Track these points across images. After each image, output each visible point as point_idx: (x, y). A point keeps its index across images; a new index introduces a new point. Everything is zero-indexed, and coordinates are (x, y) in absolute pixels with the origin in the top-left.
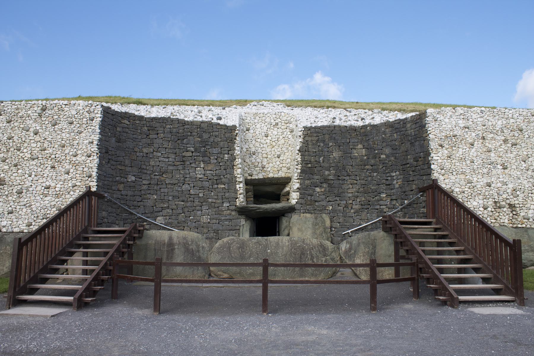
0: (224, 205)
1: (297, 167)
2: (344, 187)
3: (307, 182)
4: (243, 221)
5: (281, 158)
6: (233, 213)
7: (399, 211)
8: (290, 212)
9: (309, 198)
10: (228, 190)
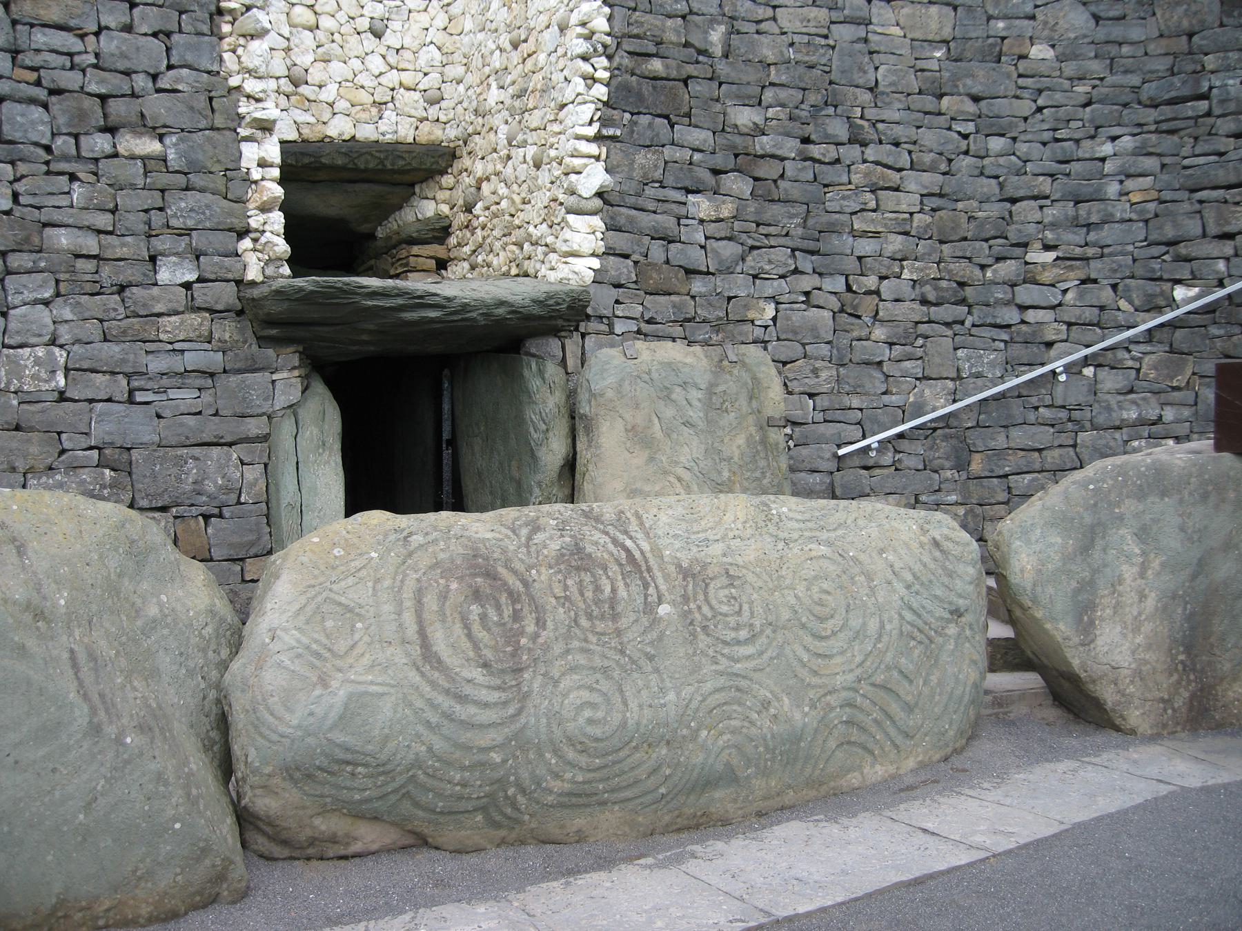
0: (164, 275)
1: (587, 68)
2: (833, 200)
3: (643, 159)
4: (285, 381)
5: (391, 39)
6: (226, 330)
7: (1133, 341)
8: (555, 332)
9: (657, 251)
10: (188, 177)
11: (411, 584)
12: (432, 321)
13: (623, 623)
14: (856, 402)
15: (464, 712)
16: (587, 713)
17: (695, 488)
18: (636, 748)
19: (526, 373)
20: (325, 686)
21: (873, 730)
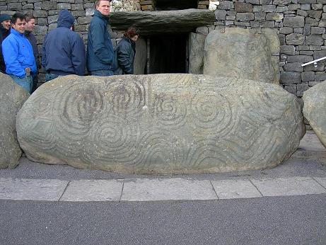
0: (87, 14)
11: (68, 94)
12: (150, 23)
13: (128, 110)
14: (311, 48)
15: (72, 130)
16: (108, 135)
17: (242, 75)
18: (124, 147)
19: (192, 37)
20: (34, 118)
21: (225, 155)
